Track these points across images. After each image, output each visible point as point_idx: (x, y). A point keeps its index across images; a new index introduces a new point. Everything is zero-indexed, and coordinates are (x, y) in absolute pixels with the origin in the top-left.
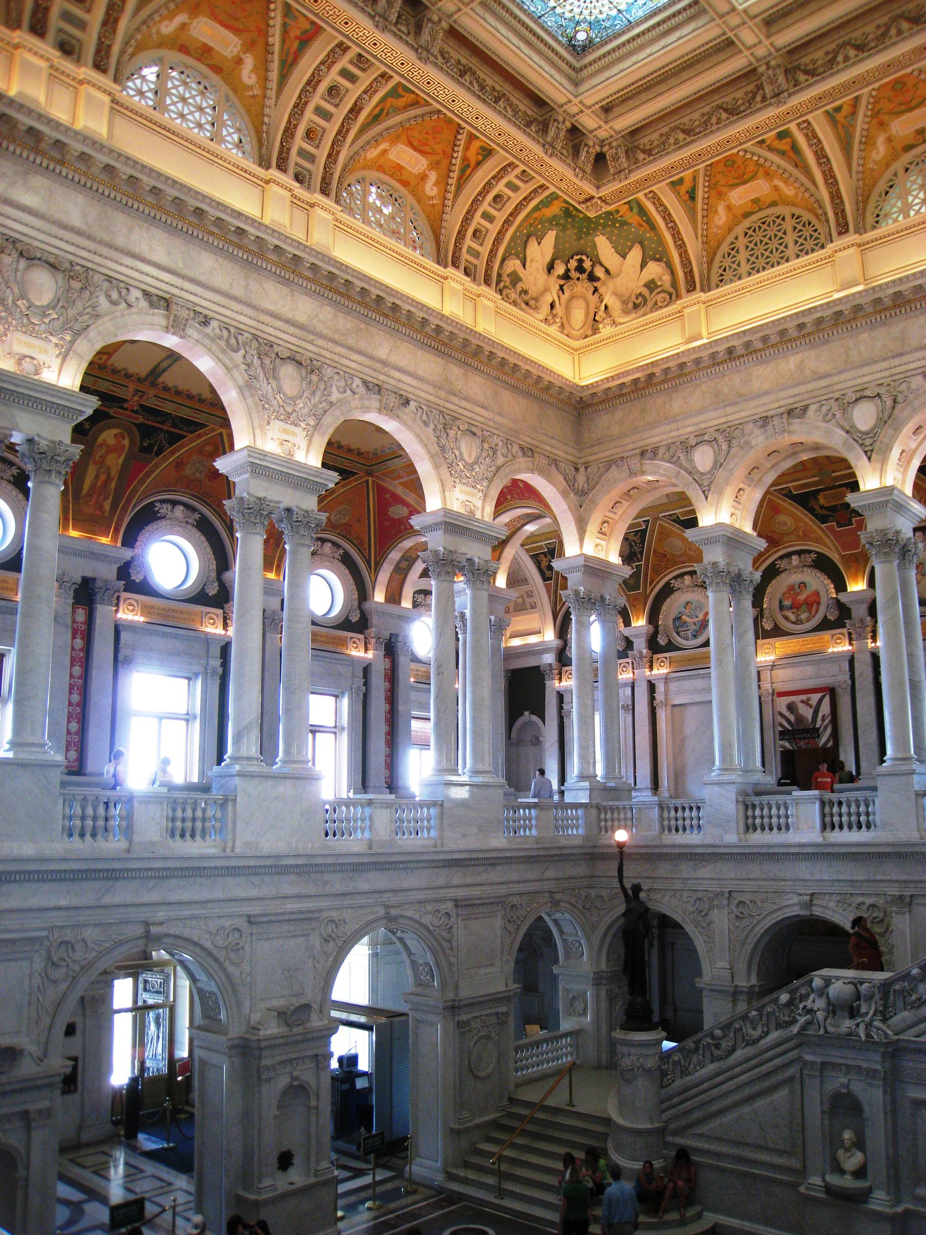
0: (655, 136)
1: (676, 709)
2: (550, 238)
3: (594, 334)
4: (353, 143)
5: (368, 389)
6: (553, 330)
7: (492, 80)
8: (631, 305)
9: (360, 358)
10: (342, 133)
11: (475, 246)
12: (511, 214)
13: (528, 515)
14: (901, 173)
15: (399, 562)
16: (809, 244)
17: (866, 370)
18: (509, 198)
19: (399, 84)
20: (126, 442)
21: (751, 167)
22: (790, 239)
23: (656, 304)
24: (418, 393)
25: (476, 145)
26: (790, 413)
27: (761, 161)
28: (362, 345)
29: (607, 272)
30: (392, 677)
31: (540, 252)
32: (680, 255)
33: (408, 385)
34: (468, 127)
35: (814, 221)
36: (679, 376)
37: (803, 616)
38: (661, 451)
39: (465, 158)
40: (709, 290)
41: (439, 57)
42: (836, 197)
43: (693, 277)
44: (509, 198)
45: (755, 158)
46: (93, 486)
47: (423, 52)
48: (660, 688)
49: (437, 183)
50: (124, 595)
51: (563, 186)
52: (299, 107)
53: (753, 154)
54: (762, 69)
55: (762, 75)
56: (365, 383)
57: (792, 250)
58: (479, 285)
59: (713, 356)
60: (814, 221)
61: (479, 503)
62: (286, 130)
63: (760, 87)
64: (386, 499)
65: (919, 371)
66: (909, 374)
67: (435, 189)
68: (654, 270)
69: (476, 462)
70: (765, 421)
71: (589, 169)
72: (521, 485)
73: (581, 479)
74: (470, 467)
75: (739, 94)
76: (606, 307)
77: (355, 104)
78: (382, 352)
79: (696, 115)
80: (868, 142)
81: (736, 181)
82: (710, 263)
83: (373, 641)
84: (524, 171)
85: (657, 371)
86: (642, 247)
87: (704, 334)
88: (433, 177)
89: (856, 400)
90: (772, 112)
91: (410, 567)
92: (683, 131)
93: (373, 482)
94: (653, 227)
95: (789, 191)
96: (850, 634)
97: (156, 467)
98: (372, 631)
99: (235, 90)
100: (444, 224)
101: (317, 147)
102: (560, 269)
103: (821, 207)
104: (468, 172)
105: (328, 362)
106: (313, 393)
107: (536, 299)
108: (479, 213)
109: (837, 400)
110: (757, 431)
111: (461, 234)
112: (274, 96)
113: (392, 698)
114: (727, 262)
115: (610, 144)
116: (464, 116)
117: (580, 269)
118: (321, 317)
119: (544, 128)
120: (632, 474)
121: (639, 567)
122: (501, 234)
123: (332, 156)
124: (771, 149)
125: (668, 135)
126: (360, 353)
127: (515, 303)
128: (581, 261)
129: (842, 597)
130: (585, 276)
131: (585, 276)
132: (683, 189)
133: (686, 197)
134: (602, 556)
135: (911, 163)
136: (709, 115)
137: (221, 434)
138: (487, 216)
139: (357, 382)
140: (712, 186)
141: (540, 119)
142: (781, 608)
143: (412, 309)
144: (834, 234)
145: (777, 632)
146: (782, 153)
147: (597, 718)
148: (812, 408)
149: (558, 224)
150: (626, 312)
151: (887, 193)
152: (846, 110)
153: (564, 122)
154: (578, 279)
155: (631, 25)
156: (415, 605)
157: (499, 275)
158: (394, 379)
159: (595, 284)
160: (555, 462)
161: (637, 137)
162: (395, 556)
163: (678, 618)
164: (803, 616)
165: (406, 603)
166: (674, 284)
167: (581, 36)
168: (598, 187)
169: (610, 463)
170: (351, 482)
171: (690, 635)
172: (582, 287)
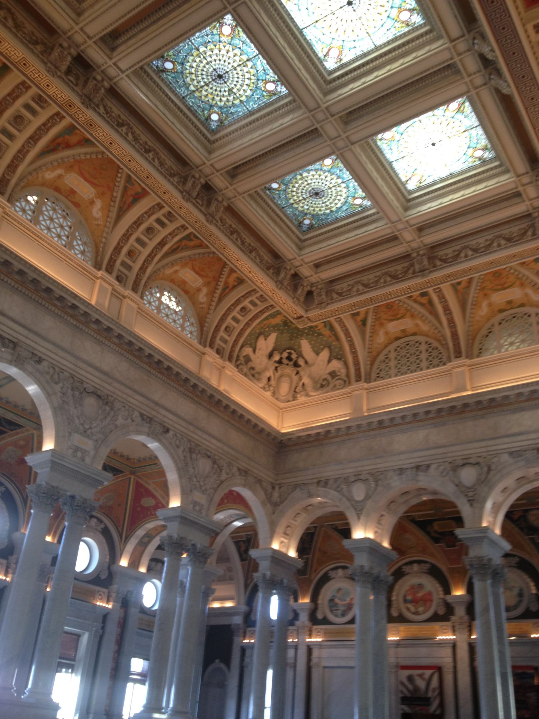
1: (327, 670)
2: (273, 337)
3: (294, 400)
4: (157, 263)
5: (143, 419)
6: (268, 394)
7: (249, 240)
8: (319, 385)
10: (151, 256)
11: (226, 337)
12: (250, 320)
13: (237, 515)
14: (496, 324)
15: (143, 537)
16: (436, 361)
18: (250, 310)
19: (192, 233)
21: (402, 311)
22: (424, 356)
23: (335, 386)
24: (176, 425)
25: (234, 275)
27: (409, 308)
29: (306, 362)
30: (123, 624)
31: (266, 345)
32: (354, 357)
34: (231, 265)
35: (440, 348)
36: (347, 434)
37: (421, 609)
38: (331, 482)
39: (226, 283)
40: (370, 382)
41: (219, 221)
42: (455, 335)
43: (360, 372)
44: (250, 310)
45: (405, 306)
47: (210, 217)
48: (316, 653)
49: (207, 295)
51: (285, 307)
52: (126, 237)
53: (404, 303)
54: (414, 255)
55: (414, 258)
56: (142, 415)
57: (424, 364)
58: (225, 361)
59: (369, 424)
60: (440, 348)
62: (116, 248)
63: (412, 265)
64: (141, 492)
65: (507, 450)
66: (500, 452)
67: (205, 298)
68: (336, 365)
70: (401, 471)
71: (302, 299)
72: (235, 494)
73: (276, 495)
75: (399, 267)
76: (303, 384)
77: (163, 240)
78: (156, 397)
79: (371, 277)
80: (476, 304)
81: (391, 318)
82: (372, 364)
83: (114, 595)
84: (262, 296)
85: (332, 429)
88: (205, 290)
89: (464, 465)
90: (418, 281)
91: (149, 542)
92: (363, 285)
93: (134, 479)
94: (338, 339)
95: (425, 328)
96: (453, 627)
98: (115, 587)
100: (208, 320)
101: (134, 262)
102: (277, 357)
103: (445, 339)
104: (227, 291)
105: (119, 398)
106: (105, 418)
107: (259, 373)
108: (231, 316)
109: (450, 463)
112: (111, 227)
113: (120, 642)
114: (383, 366)
115: (317, 286)
116: (229, 258)
117: (289, 358)
119: (277, 272)
120: (310, 496)
121: (307, 559)
122: (243, 330)
123: (143, 269)
124: (415, 301)
125: (353, 286)
126: (142, 395)
127: (245, 375)
128: (290, 354)
129: (448, 598)
130: (292, 363)
131: (292, 363)
132: (359, 318)
133: (360, 323)
134: (284, 550)
135: (503, 320)
136: (380, 278)
137: (33, 434)
138: (235, 319)
139: (136, 414)
140: (377, 319)
141: (276, 266)
142: (406, 601)
143: (181, 372)
144: (452, 356)
145: (401, 619)
146: (422, 305)
147: (270, 674)
148: (434, 466)
149: (279, 330)
150: (315, 389)
151: (487, 336)
152: (464, 285)
153: (290, 269)
154: (287, 364)
155: (337, 220)
156: (149, 569)
157: (238, 356)
159: (298, 369)
160: (259, 481)
161: (334, 284)
162: (140, 532)
163: (331, 600)
164: (421, 609)
165: (143, 570)
166: (348, 375)
167: (307, 222)
168: (307, 311)
169: (296, 486)
170: (118, 478)
171: (339, 612)
172: (289, 370)
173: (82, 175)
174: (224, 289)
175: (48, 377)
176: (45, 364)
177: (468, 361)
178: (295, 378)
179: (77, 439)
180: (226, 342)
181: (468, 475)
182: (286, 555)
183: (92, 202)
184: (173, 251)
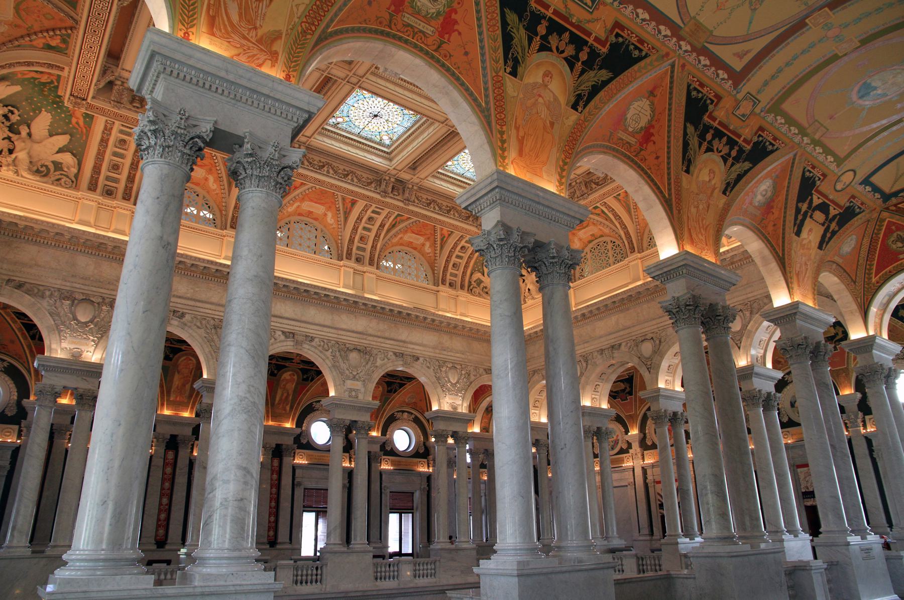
9: (392, 342)
10: (377, 236)
17: (646, 325)
20: (295, 377)
22: (610, 254)
26: (613, 347)
28: (393, 335)
33: (418, 350)
42: (627, 234)
46: (281, 399)
49: (430, 247)
50: (298, 451)
52: (355, 229)
56: (395, 354)
61: (460, 402)
62: (350, 240)
69: (457, 382)
70: (602, 351)
74: (454, 385)
88: (428, 244)
95: (607, 231)
97: (311, 387)
99: (325, 227)
110: (599, 357)
118: (371, 325)
126: (391, 339)
127: (480, 295)
138: (458, 257)
148: (624, 344)
157: (470, 282)
158: (410, 349)
173: (312, 201)
174: (442, 240)
175: (320, 348)
176: (316, 340)
177: (639, 255)
179: (350, 384)
180: (456, 276)
181: (647, 348)
182: (540, 423)
183: (325, 215)
184: (393, 226)
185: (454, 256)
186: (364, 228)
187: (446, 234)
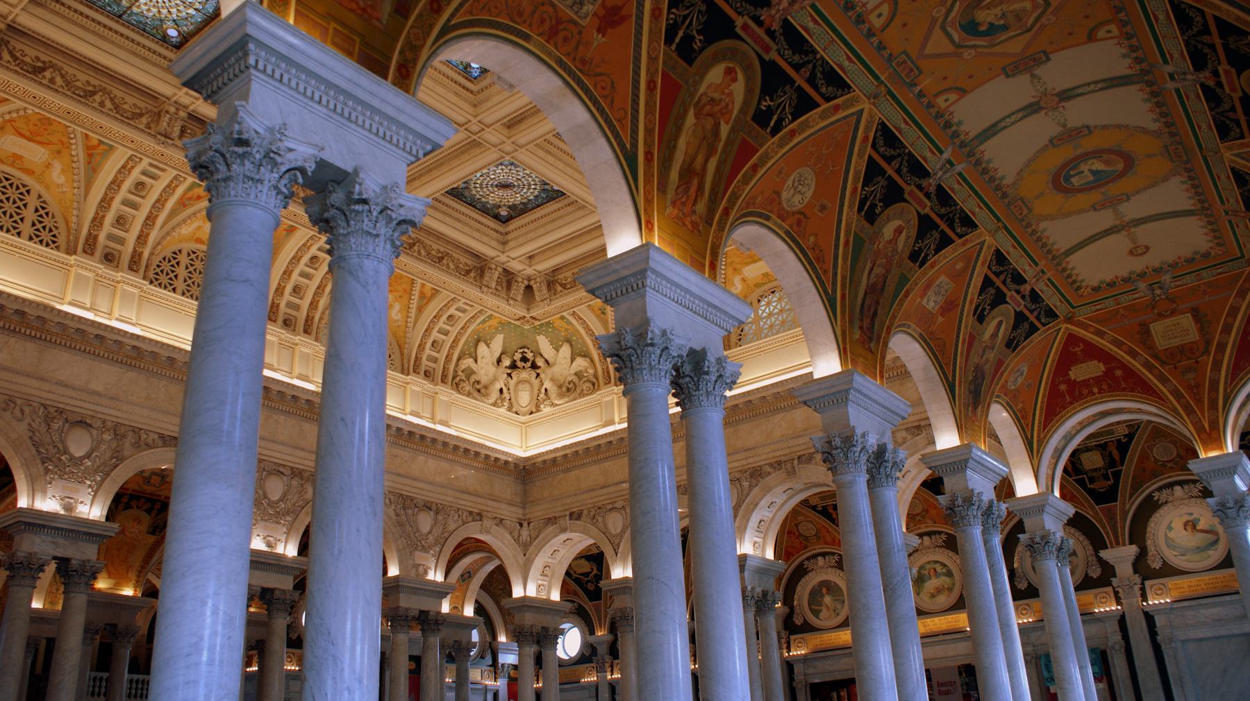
0: (569, 274)
6: (503, 410)
8: (564, 389)
68: (581, 363)
86: (571, 345)
87: (617, 419)
102: (507, 362)
107: (486, 387)
111: (421, 347)
117: (524, 359)
127: (469, 395)
130: (529, 364)
150: (561, 396)
157: (455, 371)
160: (500, 522)
166: (596, 376)
172: (526, 374)
178: (536, 382)
180: (435, 360)
182: (548, 601)
185: (436, 329)
186: (303, 275)
187: (428, 293)
